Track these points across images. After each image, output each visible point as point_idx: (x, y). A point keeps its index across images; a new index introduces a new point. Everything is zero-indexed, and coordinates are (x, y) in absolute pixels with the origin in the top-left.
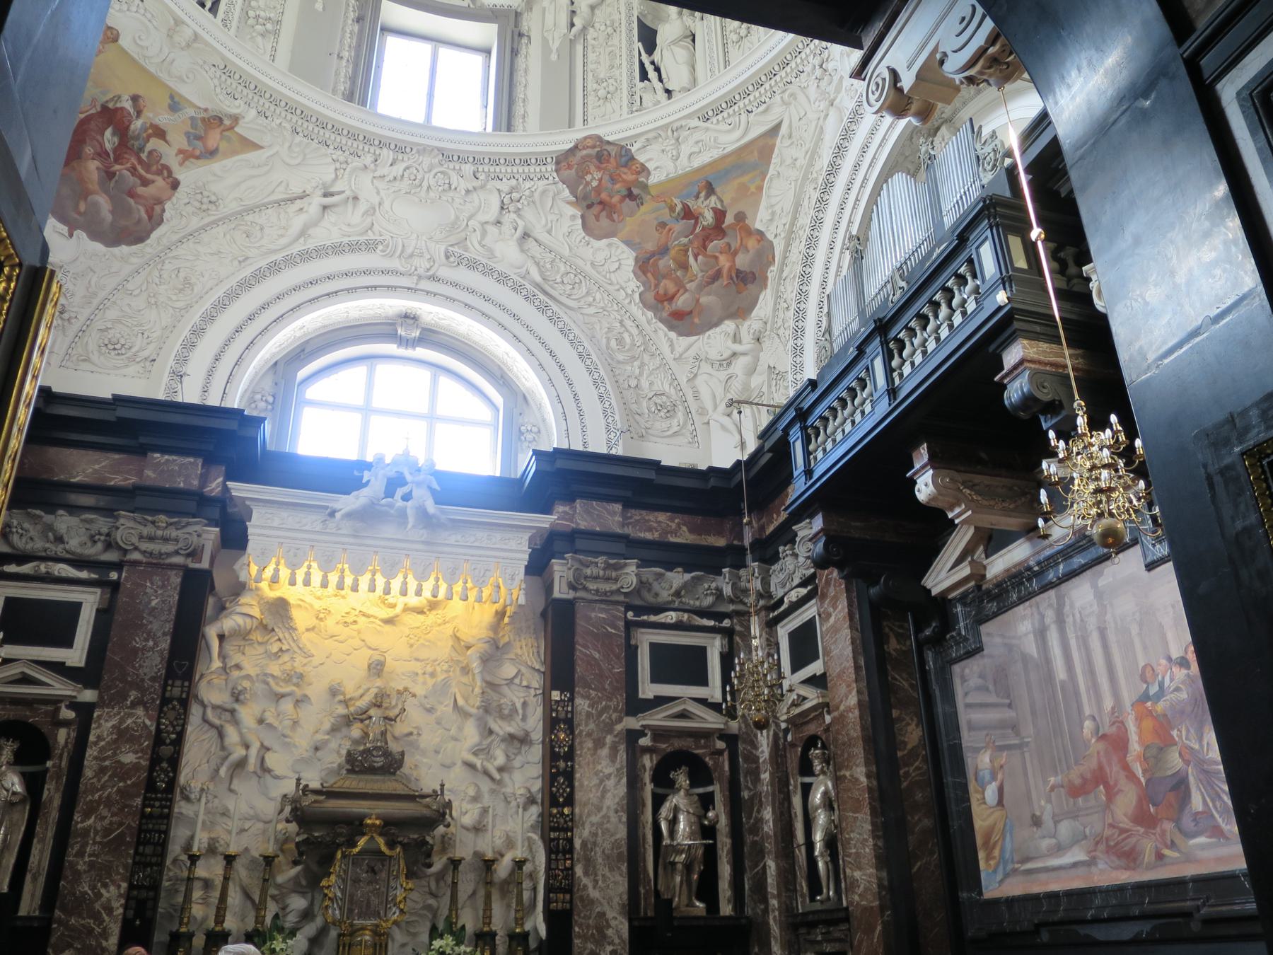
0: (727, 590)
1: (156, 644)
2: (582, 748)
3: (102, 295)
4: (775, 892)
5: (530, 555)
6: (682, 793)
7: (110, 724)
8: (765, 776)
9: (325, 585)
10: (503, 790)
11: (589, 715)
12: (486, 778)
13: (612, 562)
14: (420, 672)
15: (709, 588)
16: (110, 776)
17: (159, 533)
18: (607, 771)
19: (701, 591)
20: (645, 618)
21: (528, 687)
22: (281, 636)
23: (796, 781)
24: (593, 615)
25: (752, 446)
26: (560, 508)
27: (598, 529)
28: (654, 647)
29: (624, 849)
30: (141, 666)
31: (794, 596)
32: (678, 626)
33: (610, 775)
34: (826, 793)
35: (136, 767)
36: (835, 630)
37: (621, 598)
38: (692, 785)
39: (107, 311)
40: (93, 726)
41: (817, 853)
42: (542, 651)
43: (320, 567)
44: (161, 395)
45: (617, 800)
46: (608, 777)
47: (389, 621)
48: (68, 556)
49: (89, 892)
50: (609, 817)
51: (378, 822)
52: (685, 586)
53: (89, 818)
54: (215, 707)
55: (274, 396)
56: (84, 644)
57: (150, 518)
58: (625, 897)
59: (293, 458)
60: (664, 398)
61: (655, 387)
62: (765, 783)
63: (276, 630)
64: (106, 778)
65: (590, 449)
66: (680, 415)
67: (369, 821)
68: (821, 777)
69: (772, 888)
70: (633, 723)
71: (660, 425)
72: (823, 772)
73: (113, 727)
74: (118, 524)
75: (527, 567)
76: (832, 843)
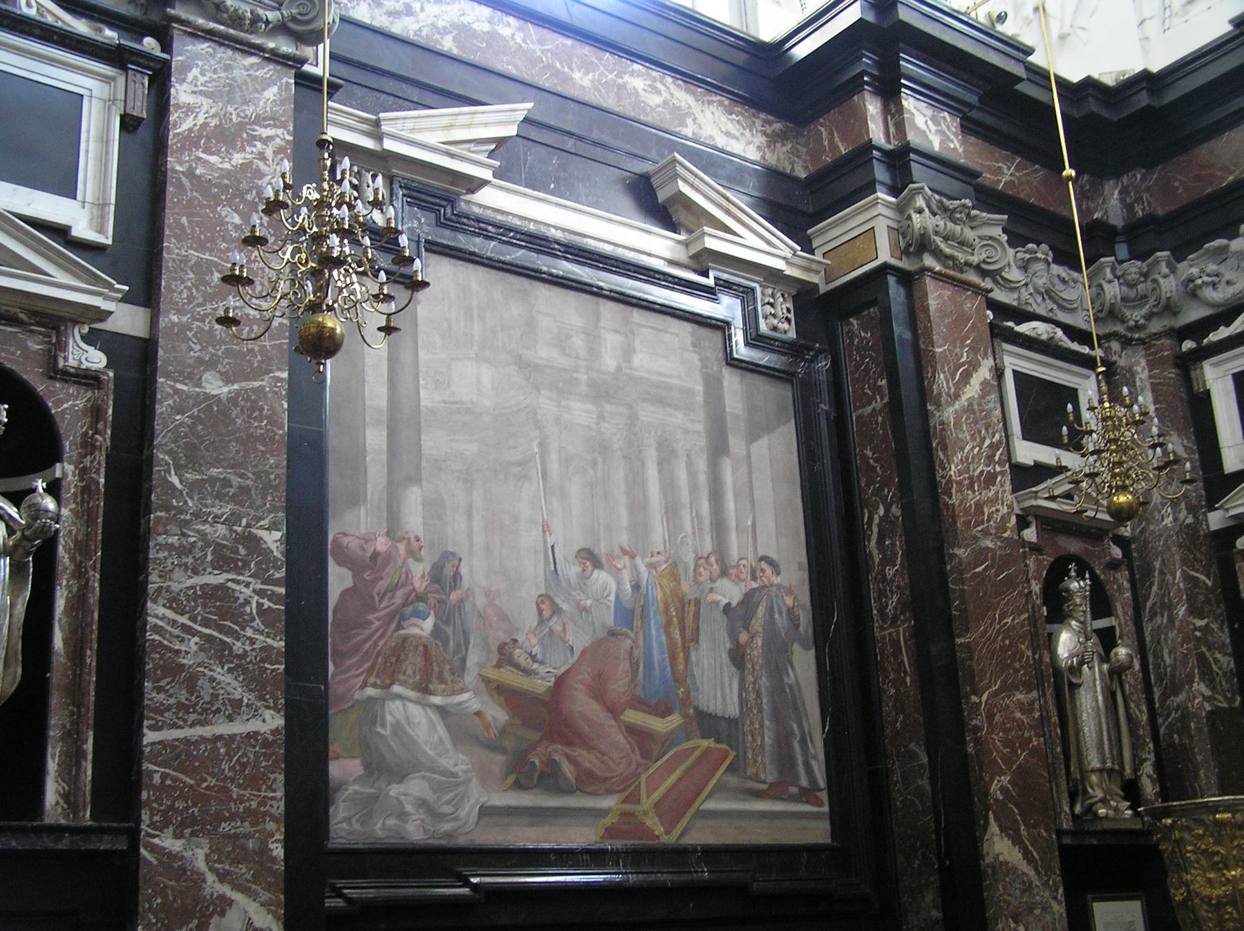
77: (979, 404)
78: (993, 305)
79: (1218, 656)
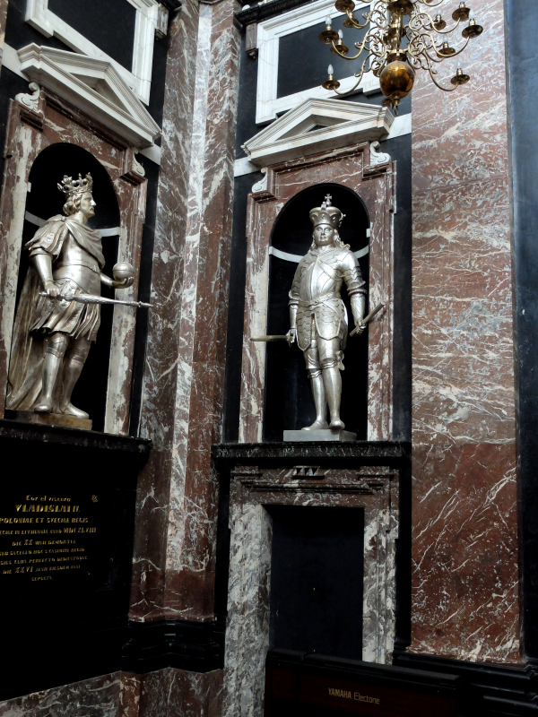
8: (193, 240)
69: (182, 403)
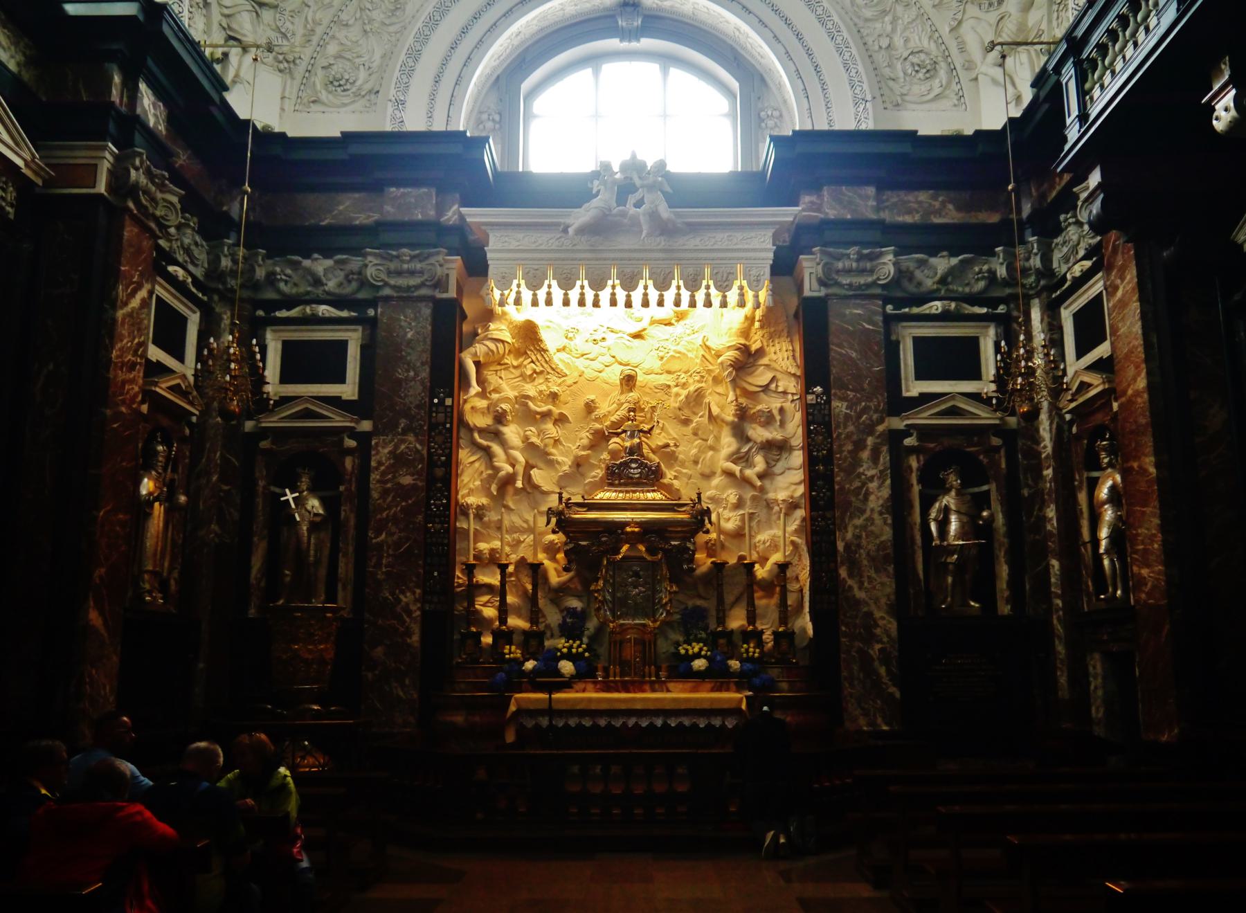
0: (1002, 272)
1: (417, 374)
2: (841, 452)
3: (319, 30)
4: (1059, 592)
5: (775, 253)
6: (953, 493)
7: (386, 451)
8: (1048, 473)
9: (566, 303)
10: (766, 497)
11: (847, 417)
12: (748, 487)
13: (866, 251)
14: (672, 384)
15: (980, 272)
16: (393, 497)
17: (405, 266)
18: (870, 473)
19: (971, 276)
20: (907, 310)
21: (785, 393)
22: (534, 358)
23: (1081, 476)
24: (848, 312)
25: (1028, 95)
26: (806, 199)
27: (849, 217)
28: (917, 341)
29: (890, 551)
30: (406, 396)
31: (1077, 270)
32: (945, 317)
33: (873, 477)
34: (1113, 488)
35: (414, 487)
36: (1123, 304)
37: (878, 291)
38: (965, 485)
39: (328, 47)
40: (373, 452)
41: (1102, 551)
42: (798, 355)
43: (560, 286)
44: (388, 128)
45: (881, 502)
46: (871, 479)
47: (638, 336)
48: (329, 297)
49: (390, 597)
50: (873, 519)
51: (636, 530)
52: (951, 272)
53: (381, 534)
54: (481, 431)
55: (500, 114)
56: (355, 377)
57: (394, 253)
58: (893, 597)
59: (527, 175)
60: (922, 56)
61: (911, 44)
62: (1048, 479)
63: (529, 352)
64: (390, 499)
65: (837, 127)
66: (942, 73)
67: (628, 529)
68: (1109, 470)
70: (898, 423)
71: (918, 89)
72: (1110, 465)
73: (390, 452)
74: (367, 262)
75: (772, 267)
76: (1117, 537)
77: (137, 313)
78: (158, 248)
79: (232, 510)
